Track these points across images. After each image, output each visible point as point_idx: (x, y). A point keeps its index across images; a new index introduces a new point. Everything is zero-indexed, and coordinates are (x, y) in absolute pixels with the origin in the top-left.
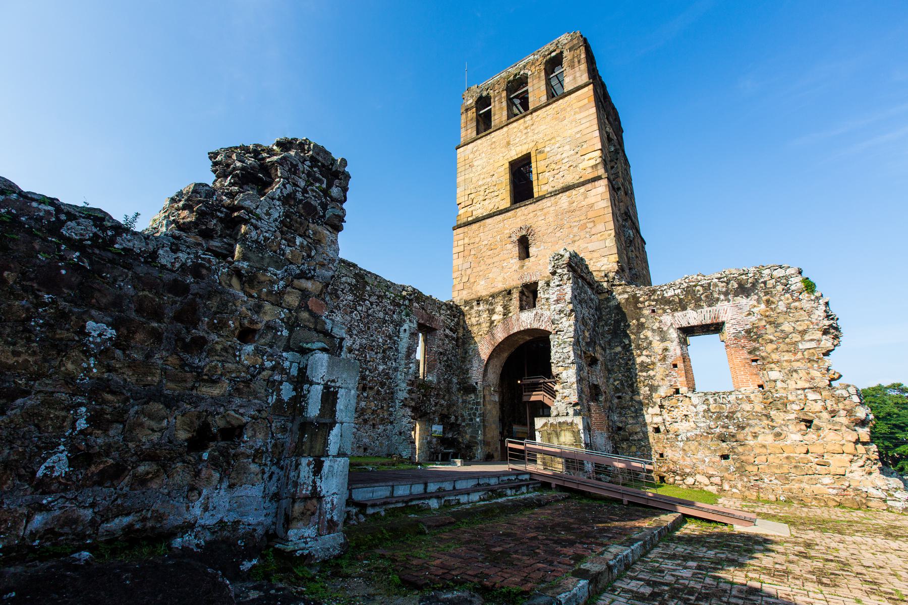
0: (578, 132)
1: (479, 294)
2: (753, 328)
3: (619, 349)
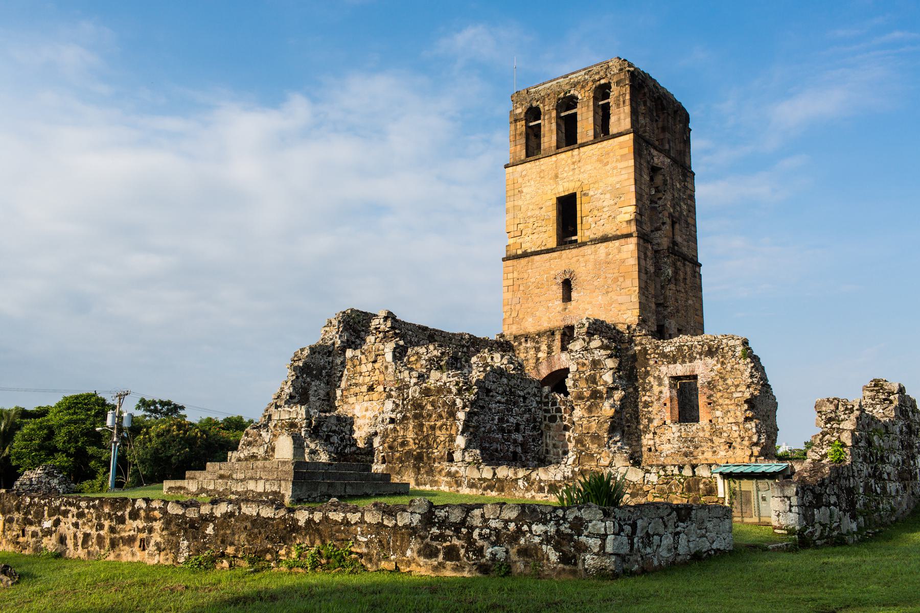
0: (618, 182)
1: (527, 331)
2: (712, 381)
3: (631, 390)
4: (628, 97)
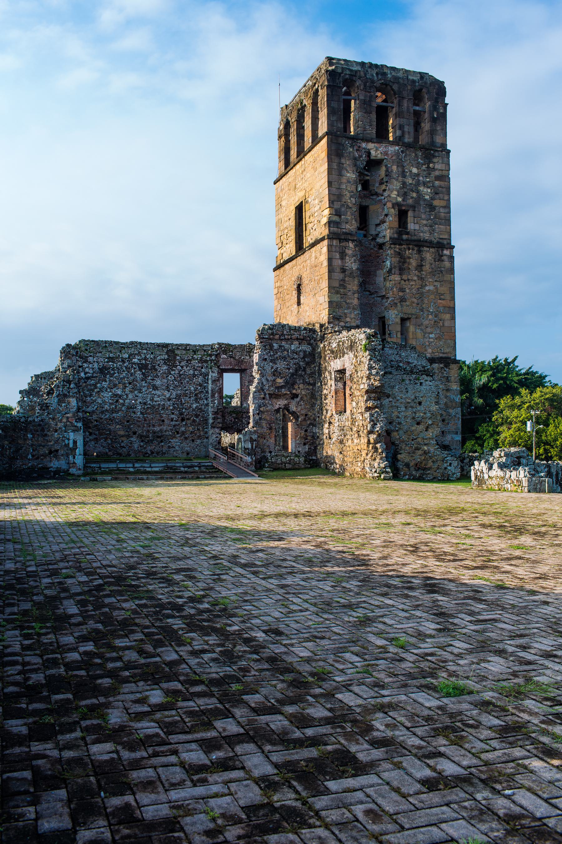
4: (326, 99)
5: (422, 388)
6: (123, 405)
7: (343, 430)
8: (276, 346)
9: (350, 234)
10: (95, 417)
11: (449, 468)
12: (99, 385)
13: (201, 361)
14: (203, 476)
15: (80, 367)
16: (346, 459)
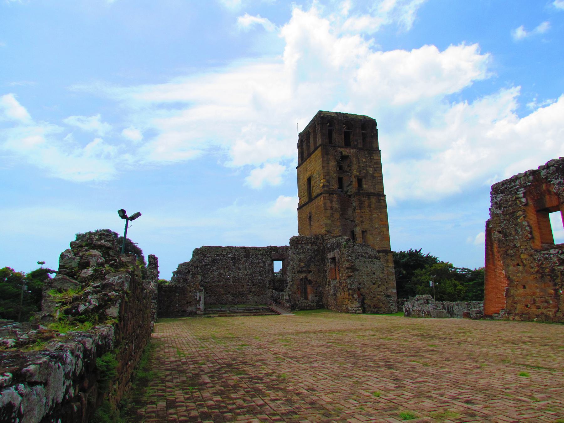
5: (375, 265)
6: (224, 278)
7: (335, 288)
8: (300, 246)
9: (334, 191)
10: (209, 285)
11: (391, 307)
12: (211, 268)
13: (262, 255)
14: (264, 314)
15: (202, 259)
16: (338, 303)
